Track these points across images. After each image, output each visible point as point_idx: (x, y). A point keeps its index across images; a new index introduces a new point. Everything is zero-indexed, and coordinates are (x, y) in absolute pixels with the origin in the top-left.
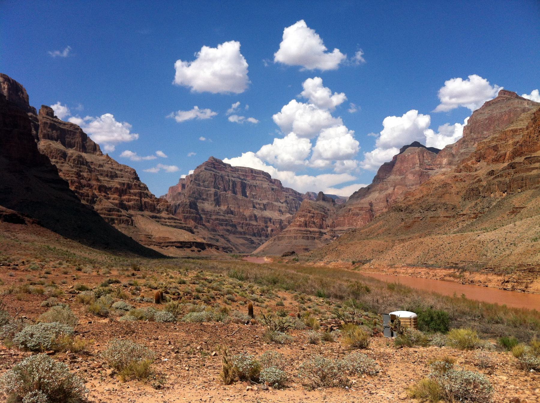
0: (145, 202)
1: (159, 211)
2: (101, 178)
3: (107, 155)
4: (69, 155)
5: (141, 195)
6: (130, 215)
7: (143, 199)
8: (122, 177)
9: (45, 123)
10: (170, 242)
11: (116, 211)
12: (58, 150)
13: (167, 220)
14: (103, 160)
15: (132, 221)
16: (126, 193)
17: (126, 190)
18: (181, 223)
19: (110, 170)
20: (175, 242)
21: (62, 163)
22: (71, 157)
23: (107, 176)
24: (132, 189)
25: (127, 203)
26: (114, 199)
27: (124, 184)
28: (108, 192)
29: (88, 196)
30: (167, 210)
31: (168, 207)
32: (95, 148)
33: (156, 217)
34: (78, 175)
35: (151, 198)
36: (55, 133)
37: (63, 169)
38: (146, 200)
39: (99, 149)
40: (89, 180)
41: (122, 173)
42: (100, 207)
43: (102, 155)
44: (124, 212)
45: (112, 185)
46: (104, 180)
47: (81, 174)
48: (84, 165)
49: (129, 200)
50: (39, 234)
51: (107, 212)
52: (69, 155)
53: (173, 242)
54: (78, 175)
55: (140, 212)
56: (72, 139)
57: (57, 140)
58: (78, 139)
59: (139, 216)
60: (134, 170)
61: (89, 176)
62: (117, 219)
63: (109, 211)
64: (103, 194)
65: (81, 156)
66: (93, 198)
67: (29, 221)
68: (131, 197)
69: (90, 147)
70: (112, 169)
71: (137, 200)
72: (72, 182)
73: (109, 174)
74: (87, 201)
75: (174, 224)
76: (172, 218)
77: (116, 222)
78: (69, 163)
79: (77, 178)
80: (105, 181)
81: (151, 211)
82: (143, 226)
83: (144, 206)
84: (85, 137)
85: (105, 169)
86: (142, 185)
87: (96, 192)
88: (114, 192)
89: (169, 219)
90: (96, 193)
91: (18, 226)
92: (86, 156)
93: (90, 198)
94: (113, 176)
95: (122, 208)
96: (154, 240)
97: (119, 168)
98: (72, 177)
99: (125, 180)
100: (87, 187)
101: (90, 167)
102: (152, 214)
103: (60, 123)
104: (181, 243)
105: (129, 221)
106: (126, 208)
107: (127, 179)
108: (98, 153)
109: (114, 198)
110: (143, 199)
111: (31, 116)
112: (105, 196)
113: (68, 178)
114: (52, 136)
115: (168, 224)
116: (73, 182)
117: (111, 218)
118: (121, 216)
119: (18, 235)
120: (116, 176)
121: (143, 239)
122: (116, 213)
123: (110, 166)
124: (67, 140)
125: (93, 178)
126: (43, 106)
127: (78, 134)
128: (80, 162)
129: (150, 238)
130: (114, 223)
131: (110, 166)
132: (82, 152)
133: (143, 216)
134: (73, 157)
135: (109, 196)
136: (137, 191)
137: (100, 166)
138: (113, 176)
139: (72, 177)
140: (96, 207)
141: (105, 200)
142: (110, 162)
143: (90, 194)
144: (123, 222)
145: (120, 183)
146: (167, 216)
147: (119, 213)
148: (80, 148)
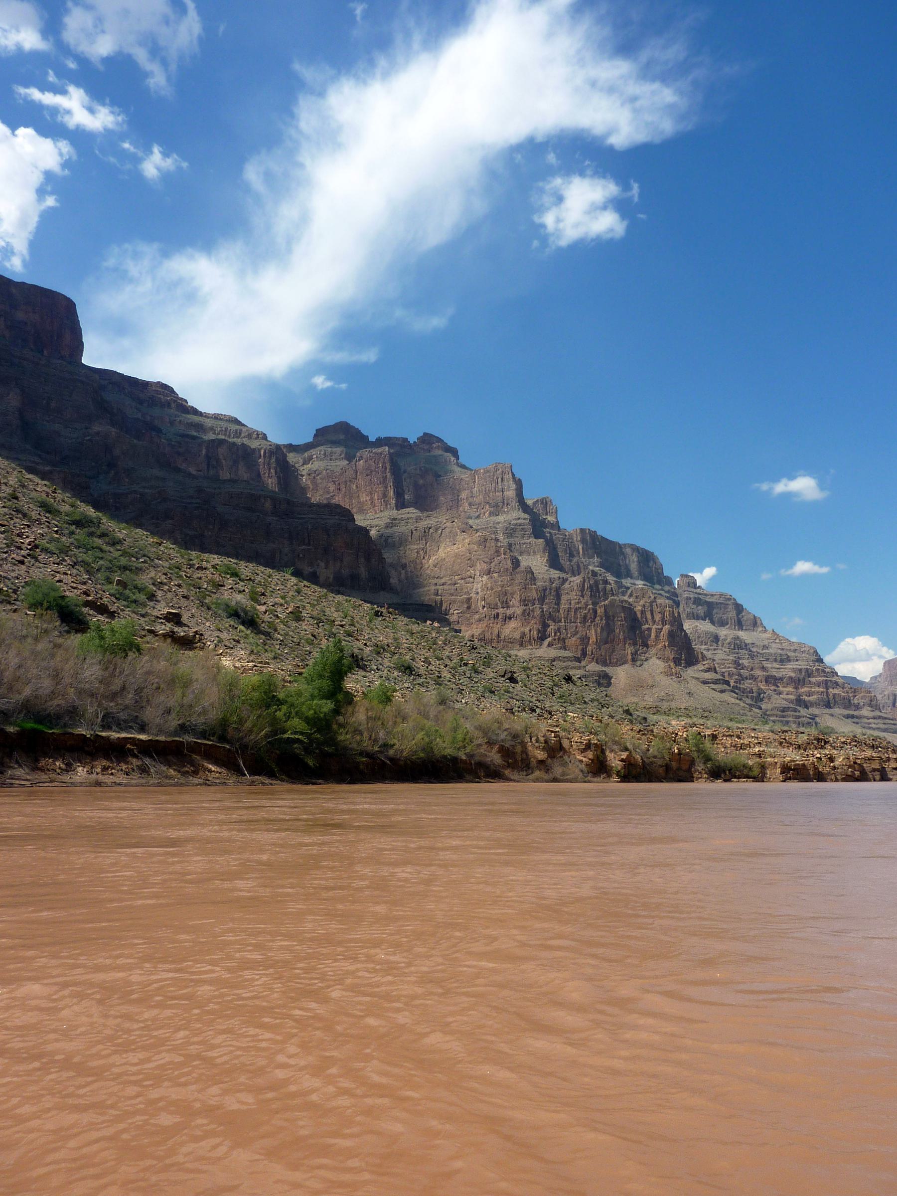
0: (834, 695)
1: (858, 707)
2: (768, 665)
5: (826, 685)
7: (830, 690)
9: (688, 599)
12: (707, 633)
14: (768, 639)
15: (816, 723)
17: (804, 679)
19: (779, 651)
21: (715, 650)
22: (725, 640)
23: (775, 660)
25: (807, 698)
27: (800, 670)
29: (751, 691)
30: (870, 705)
31: (871, 701)
32: (755, 623)
33: (853, 717)
34: (737, 664)
36: (701, 610)
37: (716, 658)
38: (836, 691)
40: (752, 669)
42: (769, 706)
43: (766, 631)
44: (803, 712)
49: (810, 694)
54: (737, 664)
55: (827, 711)
58: (732, 614)
60: (814, 648)
63: (783, 711)
64: (773, 688)
65: (738, 637)
70: (783, 649)
71: (822, 692)
73: (779, 659)
74: (752, 698)
75: (886, 726)
76: (880, 717)
80: (774, 669)
81: (845, 708)
83: (832, 701)
84: (739, 608)
85: (771, 651)
87: (763, 686)
89: (874, 718)
92: (742, 634)
93: (755, 694)
94: (784, 660)
97: (792, 648)
99: (802, 665)
102: (846, 712)
103: (706, 595)
109: (788, 693)
110: (830, 690)
111: (668, 592)
112: (775, 690)
113: (724, 670)
114: (697, 616)
115: (873, 726)
118: (799, 717)
120: (788, 660)
124: (716, 618)
126: (682, 576)
127: (730, 607)
128: (738, 645)
131: (779, 646)
133: (832, 715)
134: (728, 641)
135: (781, 689)
137: (765, 647)
138: (784, 660)
140: (763, 707)
145: (794, 670)
146: (871, 714)
147: (797, 714)
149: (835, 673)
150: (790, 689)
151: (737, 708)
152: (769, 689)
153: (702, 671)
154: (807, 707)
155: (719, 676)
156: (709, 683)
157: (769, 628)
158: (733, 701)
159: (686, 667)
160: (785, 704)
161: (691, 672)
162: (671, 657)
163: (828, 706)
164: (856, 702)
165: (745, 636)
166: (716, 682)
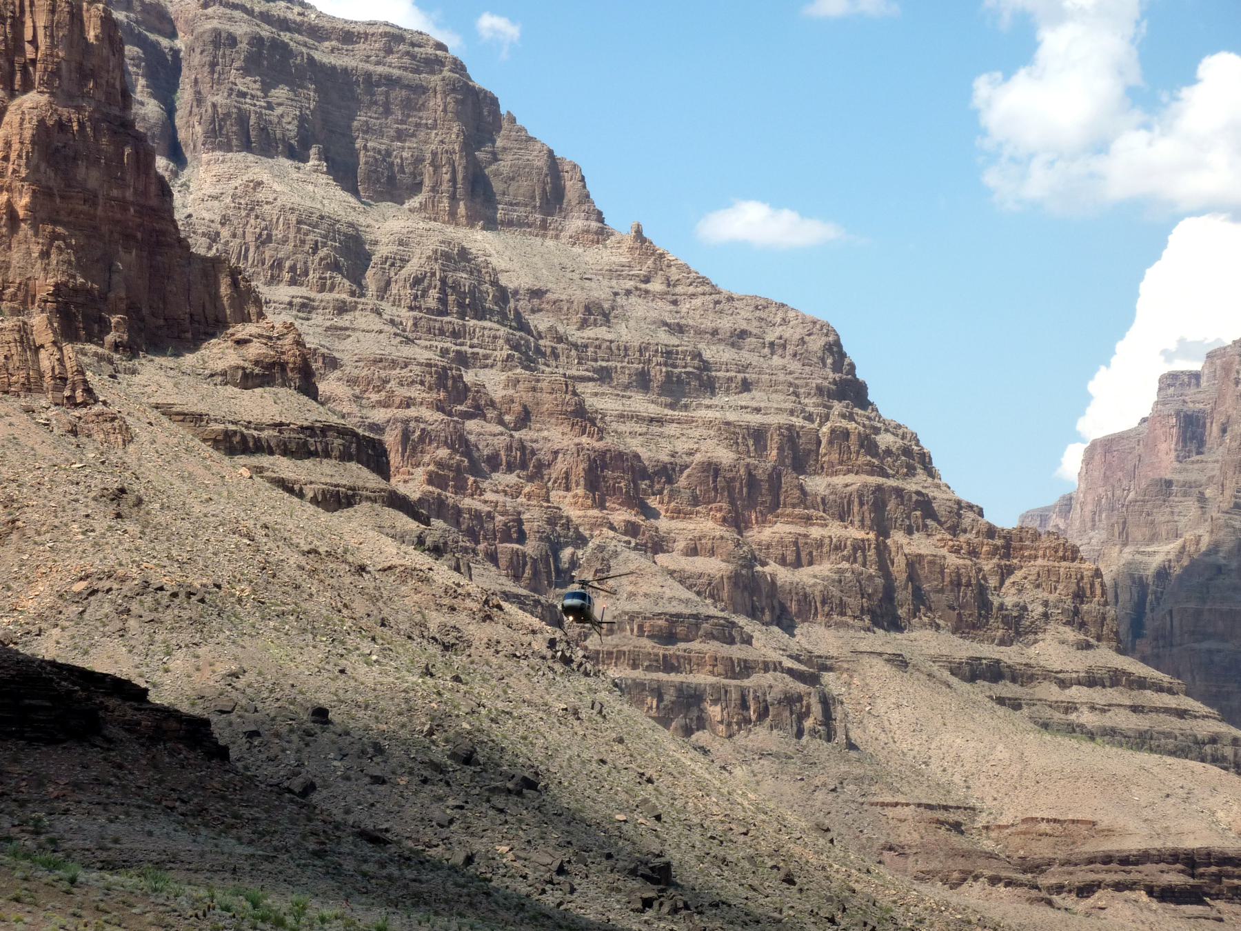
0: (914, 563)
1: (1018, 627)
3: (639, 233)
4: (382, 251)
5: (879, 510)
6: (810, 659)
7: (898, 537)
8: (746, 386)
9: (222, 41)
10: (1107, 859)
11: (710, 636)
12: (305, 221)
13: (1076, 693)
14: (614, 273)
16: (775, 505)
17: (775, 478)
18: (1181, 714)
19: (664, 337)
20: (1144, 857)
21: (342, 309)
23: (643, 381)
24: (820, 470)
25: (784, 575)
26: (693, 551)
27: (758, 435)
28: (653, 502)
30: (1075, 619)
31: (1079, 596)
33: (995, 672)
34: (450, 387)
35: (954, 530)
36: (284, 107)
37: (346, 350)
38: (921, 545)
39: (585, 198)
40: (525, 419)
41: (746, 356)
43: (602, 234)
44: (766, 642)
45: (682, 446)
46: (622, 417)
47: (469, 377)
48: (481, 314)
50: (201, 811)
51: (648, 645)
52: (382, 251)
53: (1125, 861)
54: (450, 387)
55: (880, 640)
56: (400, 136)
57: (297, 154)
58: (442, 137)
59: (879, 666)
60: (826, 329)
61: (522, 395)
62: (720, 695)
63: (669, 637)
64: (621, 516)
65: (464, 253)
66: (556, 548)
67: (131, 727)
68: (815, 532)
69: (524, 185)
70: (680, 329)
71: (859, 546)
72: (406, 436)
73: (658, 373)
76: (1116, 678)
77: (714, 712)
78: (386, 306)
79: (440, 408)
80: (632, 421)
81: (962, 628)
82: (908, 744)
83: (903, 594)
84: (479, 114)
85: (624, 333)
86: (885, 440)
87: (573, 506)
88: (695, 501)
89: (1091, 681)
90: (574, 513)
91: (59, 764)
95: (753, 614)
96: (988, 845)
97: (725, 324)
98: (408, 403)
99: (770, 409)
100: (510, 468)
101: (523, 326)
103: (317, 33)
104: (1190, 861)
105: (807, 709)
106: (782, 612)
107: (780, 400)
108: (576, 223)
110: (898, 537)
112: (632, 529)
113: (379, 415)
115: (1087, 718)
116: (413, 443)
117: (680, 689)
118: (747, 668)
119: (61, 825)
120: (705, 380)
121: (908, 835)
122: (713, 648)
123: (662, 309)
124: (367, 147)
125: (548, 401)
127: (436, 102)
128: (463, 295)
129: (957, 827)
130: (702, 723)
131: (662, 309)
132: (471, 223)
133: (900, 662)
134: (412, 268)
135: (664, 524)
136: (856, 481)
137: (595, 313)
138: (684, 381)
139: (408, 403)
141: (636, 560)
142: (656, 286)
143: (534, 518)
144: (763, 714)
146: (1077, 663)
147: (737, 652)
148: (453, 198)
149: (916, 459)
150: (707, 525)
151: (408, 599)
152: (601, 525)
153: (226, 377)
154: (784, 620)
155: (313, 414)
156: (259, 448)
157: (620, 223)
158: (391, 552)
159: (130, 349)
160: (677, 599)
161: (156, 378)
162: (45, 284)
163: (884, 614)
164: (1009, 598)
165: (502, 253)
166: (305, 443)
